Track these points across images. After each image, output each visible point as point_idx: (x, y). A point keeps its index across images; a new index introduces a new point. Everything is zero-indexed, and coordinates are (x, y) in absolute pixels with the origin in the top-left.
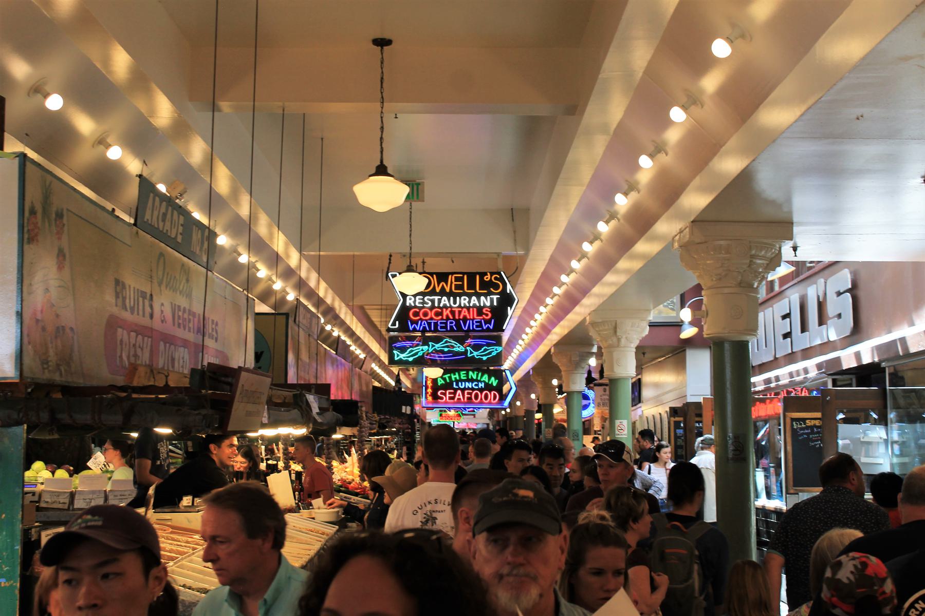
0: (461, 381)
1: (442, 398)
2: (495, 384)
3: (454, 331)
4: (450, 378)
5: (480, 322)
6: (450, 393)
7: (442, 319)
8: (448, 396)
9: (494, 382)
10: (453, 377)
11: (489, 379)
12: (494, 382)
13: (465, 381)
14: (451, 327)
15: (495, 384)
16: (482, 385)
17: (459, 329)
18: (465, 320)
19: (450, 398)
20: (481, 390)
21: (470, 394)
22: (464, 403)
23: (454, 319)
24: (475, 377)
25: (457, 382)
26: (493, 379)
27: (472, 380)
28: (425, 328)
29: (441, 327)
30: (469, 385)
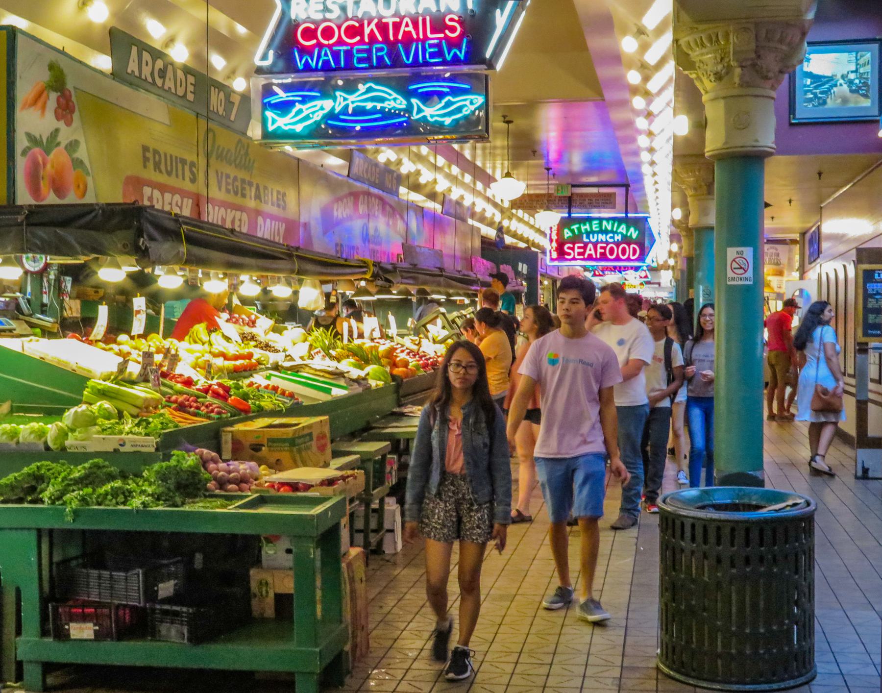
0: (593, 232)
1: (569, 254)
2: (634, 236)
3: (386, 66)
4: (579, 229)
5: (439, 46)
6: (579, 248)
7: (361, 42)
8: (577, 251)
9: (634, 233)
10: (583, 228)
11: (628, 230)
12: (634, 233)
13: (598, 233)
14: (380, 59)
15: (634, 236)
16: (618, 238)
17: (396, 62)
18: (408, 40)
19: (579, 254)
20: (618, 244)
21: (604, 248)
22: (596, 260)
23: (386, 40)
24: (609, 228)
25: (588, 234)
26: (632, 229)
27: (606, 232)
28: (326, 63)
29: (360, 60)
30: (602, 237)
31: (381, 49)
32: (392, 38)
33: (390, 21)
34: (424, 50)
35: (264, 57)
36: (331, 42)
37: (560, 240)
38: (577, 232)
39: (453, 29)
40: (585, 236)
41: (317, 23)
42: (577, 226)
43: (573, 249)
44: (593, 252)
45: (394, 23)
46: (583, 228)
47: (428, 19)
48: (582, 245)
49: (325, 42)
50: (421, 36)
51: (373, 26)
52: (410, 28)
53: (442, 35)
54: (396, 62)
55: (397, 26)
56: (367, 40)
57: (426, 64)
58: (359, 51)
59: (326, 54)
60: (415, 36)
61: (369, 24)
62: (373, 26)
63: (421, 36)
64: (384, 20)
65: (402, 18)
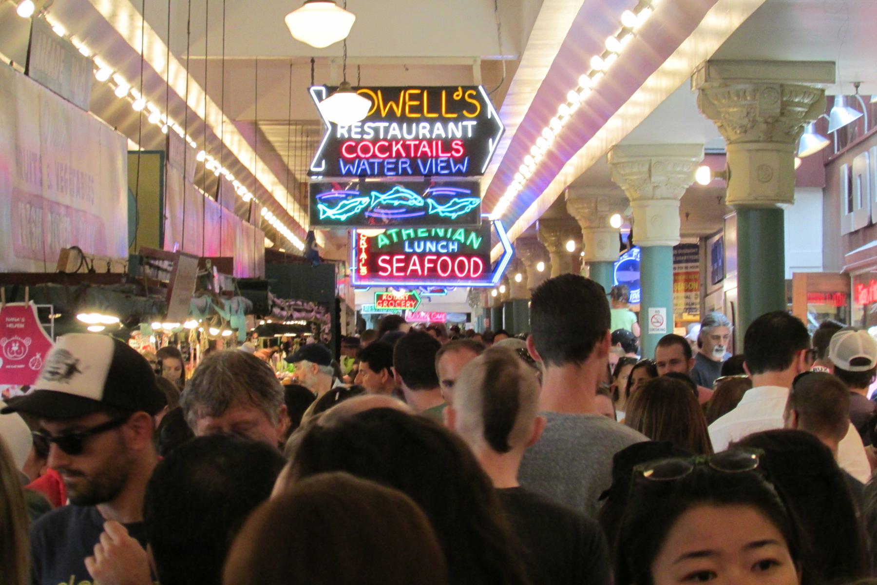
4: (399, 234)
5: (448, 162)
6: (398, 261)
7: (390, 156)
8: (395, 265)
10: (404, 233)
14: (404, 169)
17: (416, 172)
28: (364, 170)
29: (389, 170)
31: (405, 163)
32: (412, 155)
33: (412, 143)
34: (437, 165)
35: (318, 165)
36: (368, 156)
37: (373, 250)
38: (395, 239)
39: (458, 151)
40: (407, 244)
41: (358, 142)
42: (396, 230)
43: (390, 262)
44: (418, 267)
45: (415, 145)
46: (404, 233)
47: (440, 143)
48: (403, 257)
49: (363, 156)
50: (434, 154)
51: (399, 146)
52: (427, 149)
53: (449, 155)
54: (416, 172)
55: (417, 147)
56: (394, 155)
57: (437, 174)
58: (388, 163)
59: (364, 164)
60: (430, 154)
61: (396, 144)
62: (399, 146)
63: (434, 154)
64: (408, 143)
65: (421, 141)
